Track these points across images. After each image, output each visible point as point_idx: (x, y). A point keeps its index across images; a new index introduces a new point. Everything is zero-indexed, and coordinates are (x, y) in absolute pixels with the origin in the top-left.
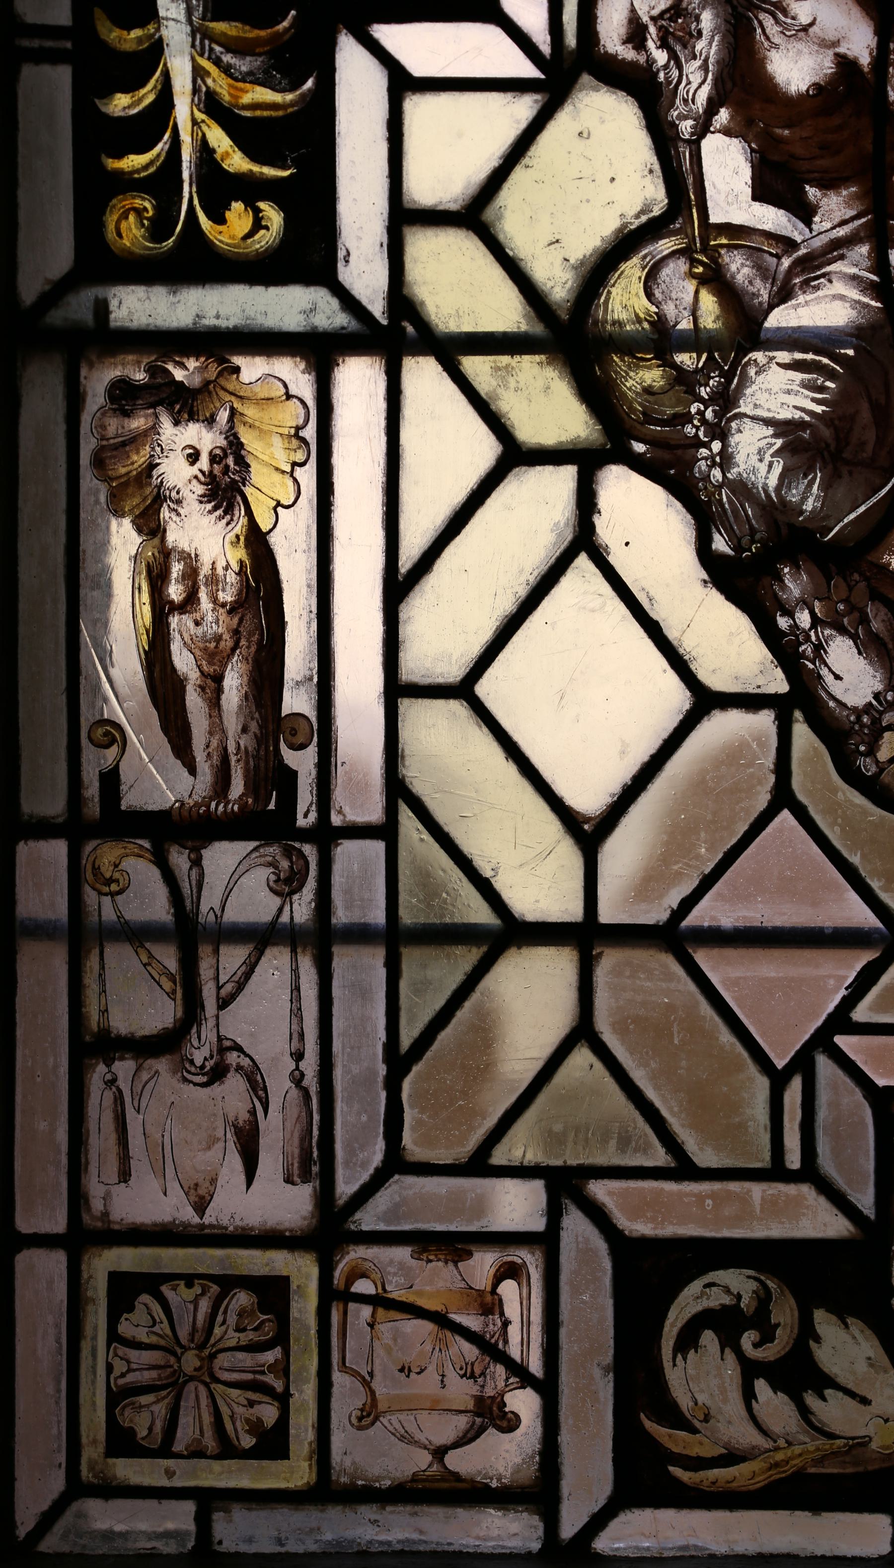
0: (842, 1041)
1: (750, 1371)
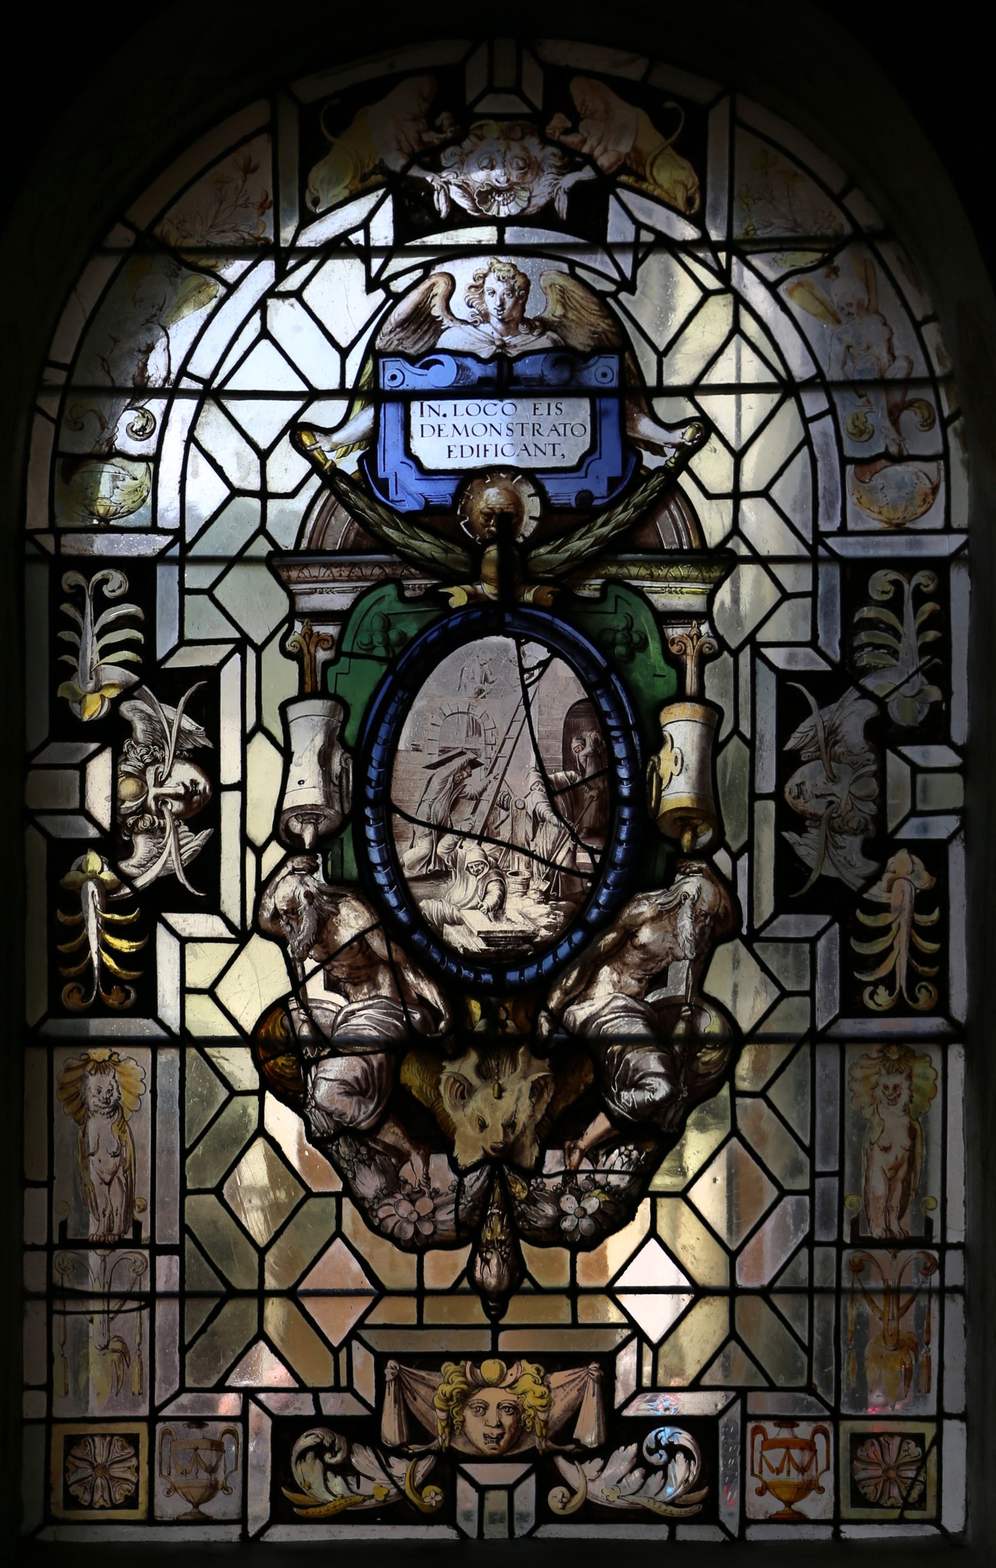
0: (364, 1334)
1: (327, 1467)
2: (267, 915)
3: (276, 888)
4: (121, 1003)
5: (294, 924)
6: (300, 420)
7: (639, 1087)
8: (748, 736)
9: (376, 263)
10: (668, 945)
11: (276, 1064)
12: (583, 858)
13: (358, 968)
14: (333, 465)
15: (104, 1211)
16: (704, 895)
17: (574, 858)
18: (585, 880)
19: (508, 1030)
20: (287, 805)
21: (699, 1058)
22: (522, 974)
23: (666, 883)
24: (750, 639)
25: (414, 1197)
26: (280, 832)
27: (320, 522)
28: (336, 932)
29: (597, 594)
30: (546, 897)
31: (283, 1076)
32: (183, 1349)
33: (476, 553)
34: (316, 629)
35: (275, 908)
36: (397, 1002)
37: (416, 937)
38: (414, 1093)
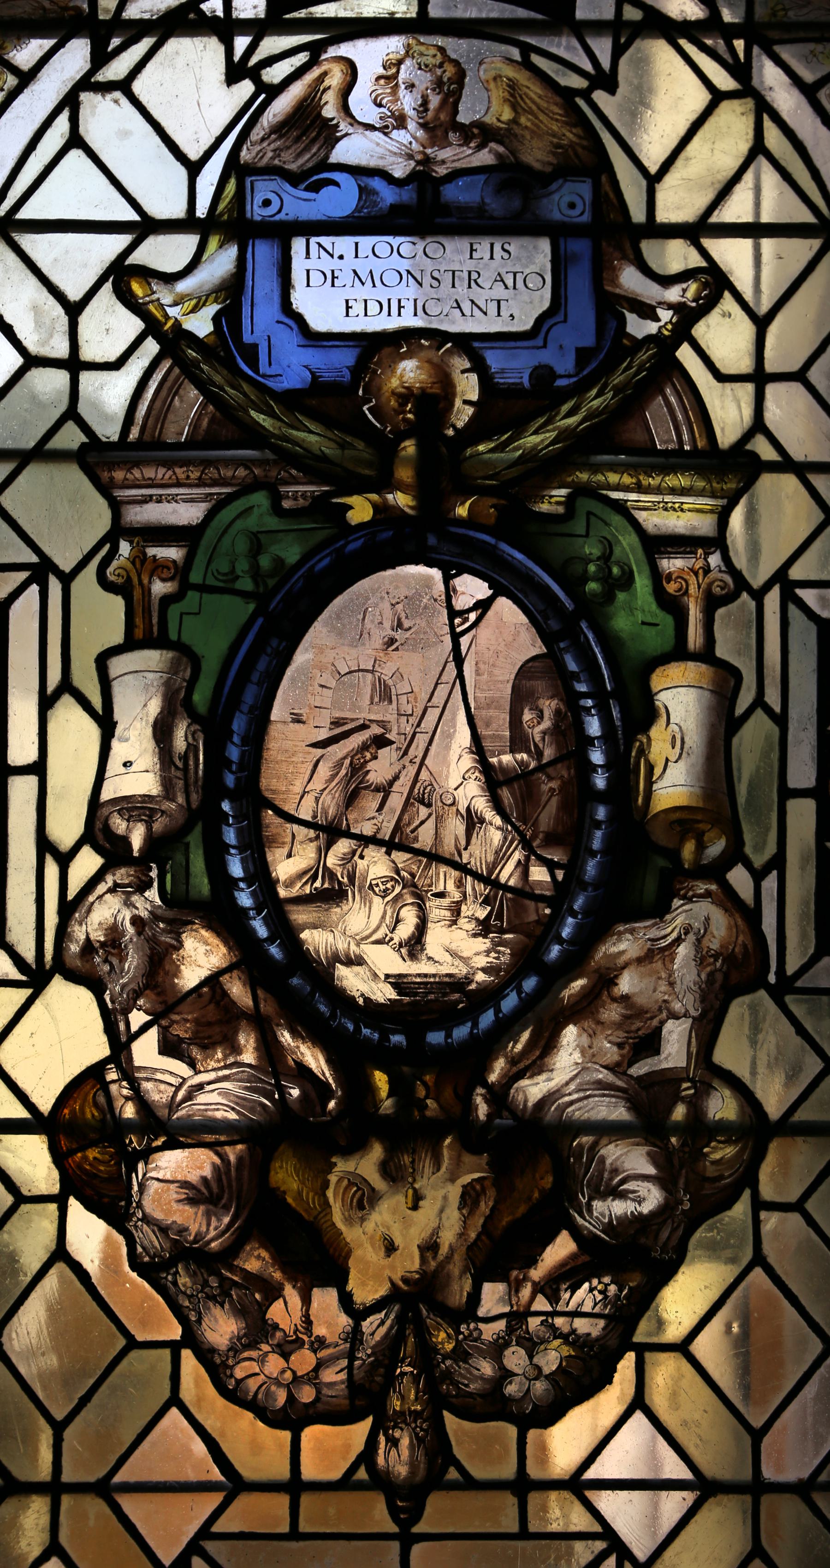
2: (74, 948)
3: (89, 911)
5: (115, 961)
6: (130, 261)
7: (618, 1194)
8: (777, 709)
9: (241, 43)
10: (660, 996)
11: (85, 1158)
12: (539, 874)
13: (209, 1024)
14: (177, 324)
16: (713, 928)
17: (525, 873)
18: (541, 905)
19: (428, 1113)
20: (107, 794)
21: (706, 1155)
22: (449, 1035)
23: (659, 910)
24: (780, 576)
25: (287, 1348)
26: (97, 833)
27: (158, 404)
28: (177, 973)
29: (561, 510)
30: (484, 928)
31: (95, 1176)
33: (387, 450)
34: (151, 551)
35: (88, 938)
36: (266, 1073)
37: (295, 981)
38: (290, 1200)
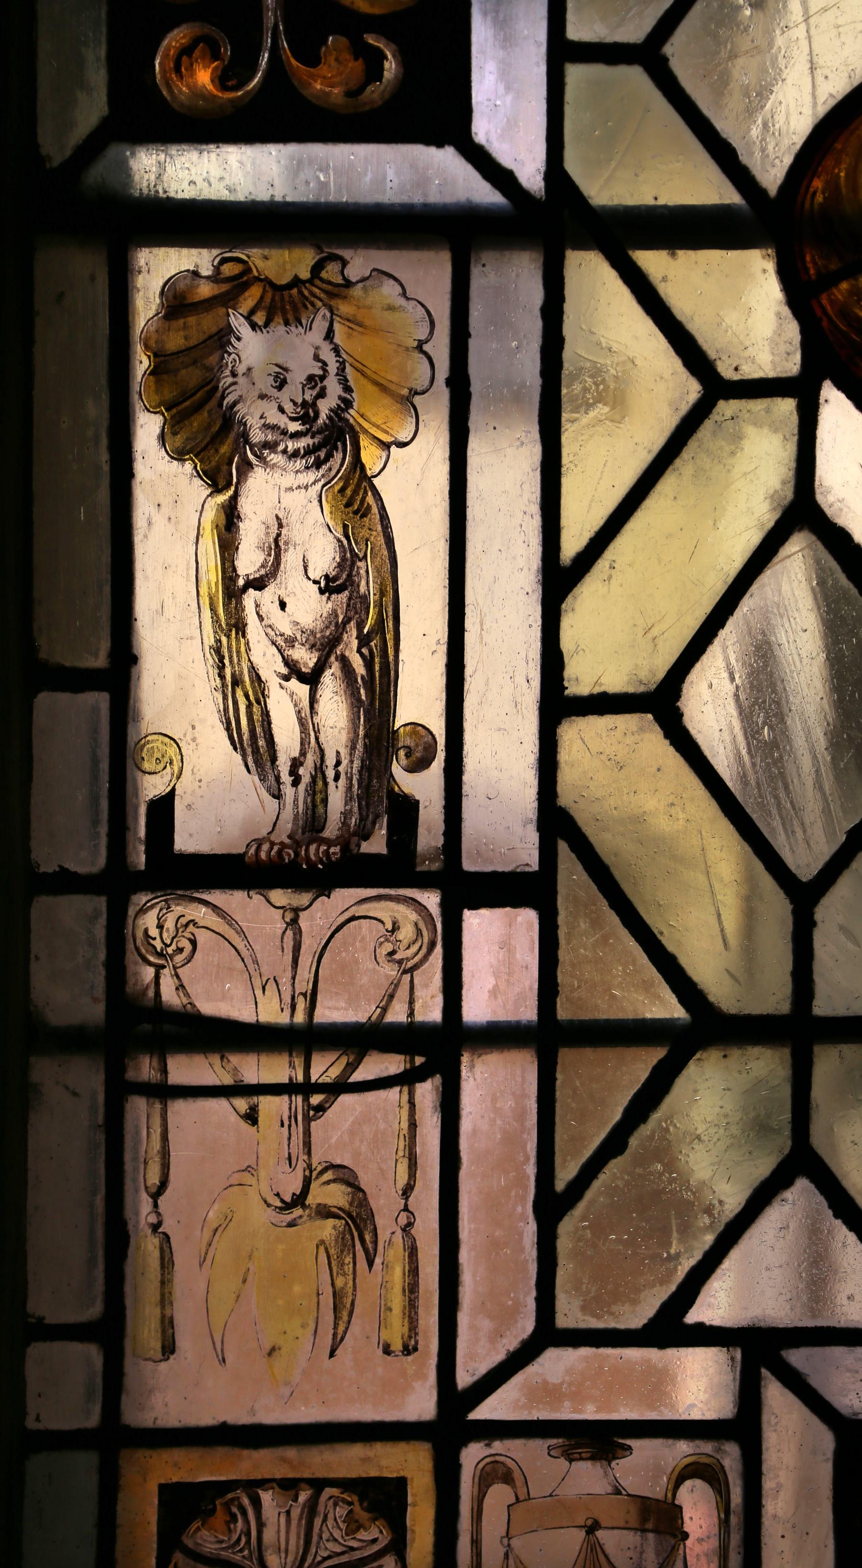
4: (353, 94)
15: (296, 764)
32: (551, 1206)
